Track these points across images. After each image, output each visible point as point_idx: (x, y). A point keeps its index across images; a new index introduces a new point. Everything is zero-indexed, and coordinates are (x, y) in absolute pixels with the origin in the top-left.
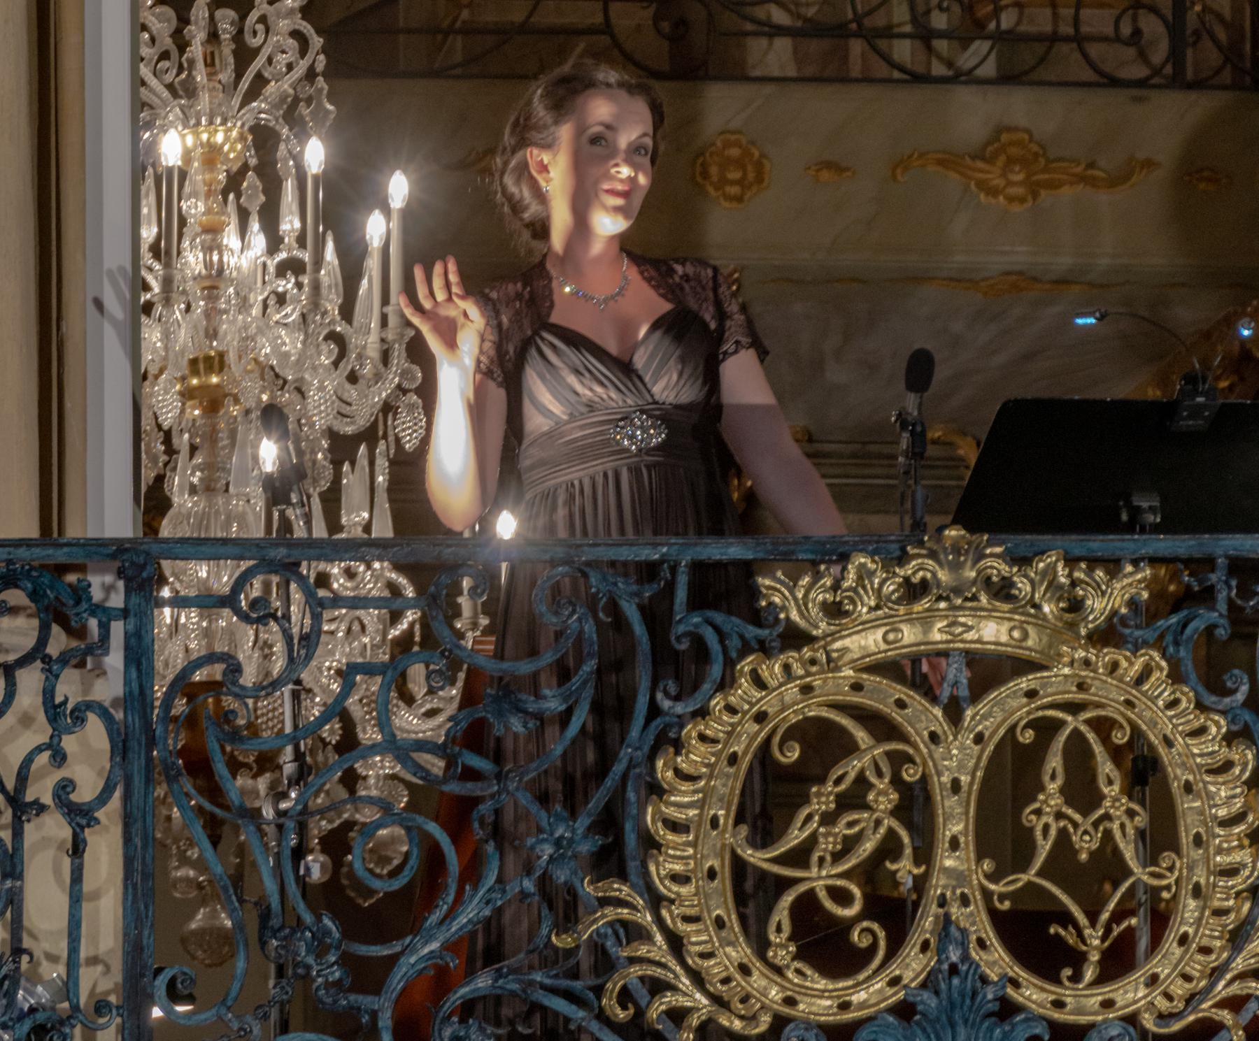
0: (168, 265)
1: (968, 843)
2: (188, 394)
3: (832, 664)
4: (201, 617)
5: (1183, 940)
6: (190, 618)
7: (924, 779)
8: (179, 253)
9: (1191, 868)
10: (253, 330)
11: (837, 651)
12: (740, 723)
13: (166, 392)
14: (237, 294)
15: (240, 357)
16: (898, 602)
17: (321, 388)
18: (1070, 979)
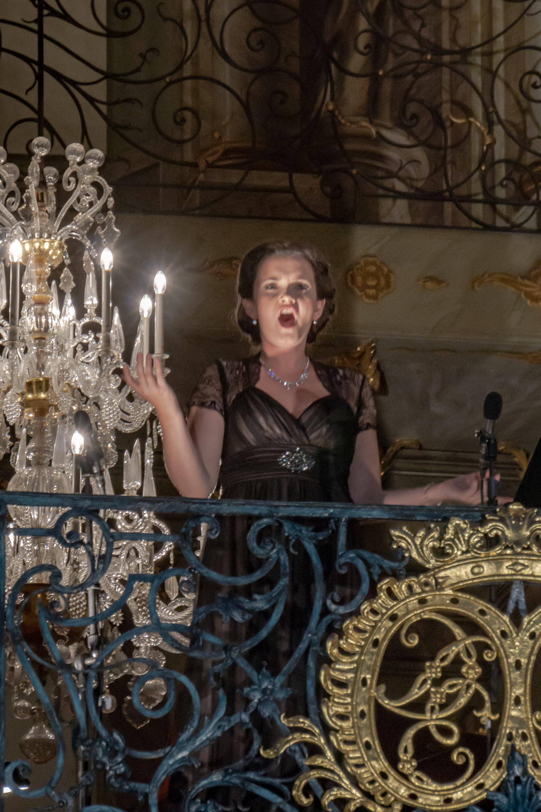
0: (13, 324)
1: (526, 700)
2: (25, 404)
3: (439, 586)
4: (34, 543)
6: (26, 543)
7: (498, 660)
8: (20, 316)
10: (67, 366)
11: (442, 578)
12: (380, 621)
13: (12, 402)
14: (57, 343)
15: (59, 382)
16: (479, 549)
17: (111, 404)
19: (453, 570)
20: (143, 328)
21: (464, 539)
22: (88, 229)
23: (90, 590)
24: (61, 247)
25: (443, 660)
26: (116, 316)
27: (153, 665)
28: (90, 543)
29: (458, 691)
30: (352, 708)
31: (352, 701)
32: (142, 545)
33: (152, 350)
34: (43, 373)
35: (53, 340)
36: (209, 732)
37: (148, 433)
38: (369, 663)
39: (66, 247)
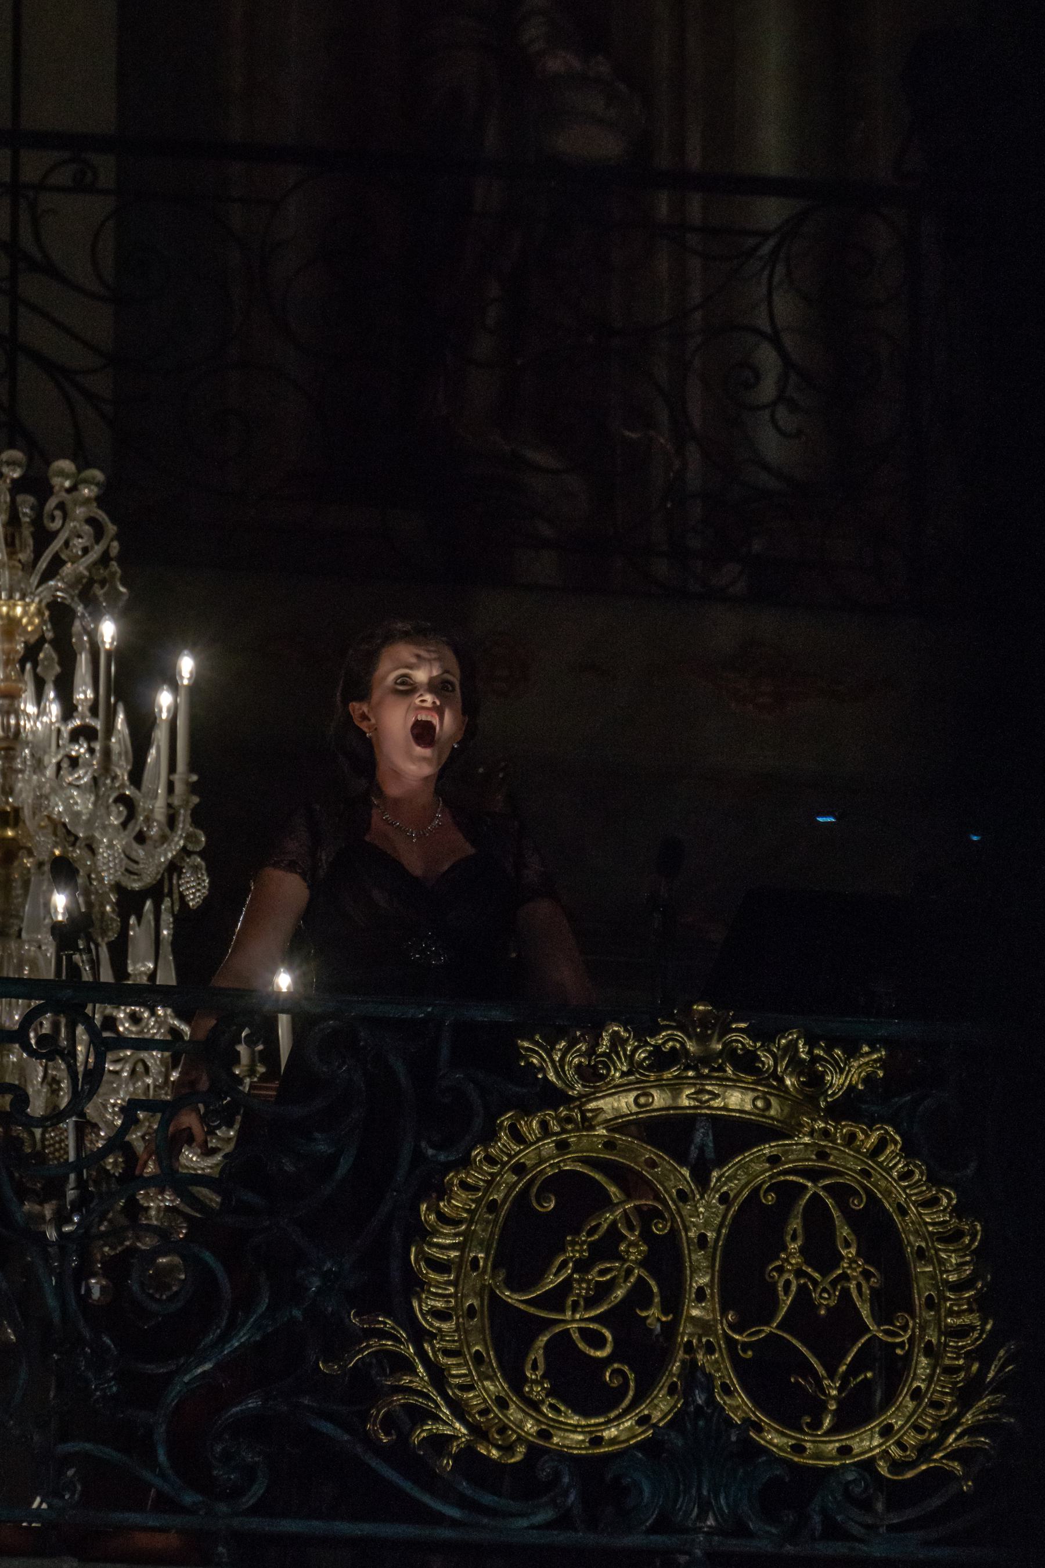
3: (587, 1124)
5: (916, 1395)
7: (674, 1233)
9: (923, 1328)
10: (47, 789)
14: (32, 755)
15: (34, 814)
16: (649, 1068)
17: (110, 846)
18: (808, 1424)
19: (608, 1099)
20: (161, 735)
21: (625, 1054)
22: (80, 587)
23: (71, 1121)
24: (39, 613)
25: (590, 1233)
26: (121, 717)
27: (163, 1234)
28: (73, 1054)
29: (613, 1279)
30: (456, 1302)
31: (456, 1292)
32: (154, 1058)
33: (172, 768)
34: (11, 800)
35: (27, 751)
36: (244, 1334)
37: (166, 890)
38: (483, 1235)
39: (47, 613)
